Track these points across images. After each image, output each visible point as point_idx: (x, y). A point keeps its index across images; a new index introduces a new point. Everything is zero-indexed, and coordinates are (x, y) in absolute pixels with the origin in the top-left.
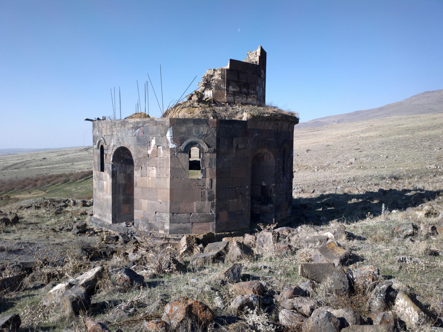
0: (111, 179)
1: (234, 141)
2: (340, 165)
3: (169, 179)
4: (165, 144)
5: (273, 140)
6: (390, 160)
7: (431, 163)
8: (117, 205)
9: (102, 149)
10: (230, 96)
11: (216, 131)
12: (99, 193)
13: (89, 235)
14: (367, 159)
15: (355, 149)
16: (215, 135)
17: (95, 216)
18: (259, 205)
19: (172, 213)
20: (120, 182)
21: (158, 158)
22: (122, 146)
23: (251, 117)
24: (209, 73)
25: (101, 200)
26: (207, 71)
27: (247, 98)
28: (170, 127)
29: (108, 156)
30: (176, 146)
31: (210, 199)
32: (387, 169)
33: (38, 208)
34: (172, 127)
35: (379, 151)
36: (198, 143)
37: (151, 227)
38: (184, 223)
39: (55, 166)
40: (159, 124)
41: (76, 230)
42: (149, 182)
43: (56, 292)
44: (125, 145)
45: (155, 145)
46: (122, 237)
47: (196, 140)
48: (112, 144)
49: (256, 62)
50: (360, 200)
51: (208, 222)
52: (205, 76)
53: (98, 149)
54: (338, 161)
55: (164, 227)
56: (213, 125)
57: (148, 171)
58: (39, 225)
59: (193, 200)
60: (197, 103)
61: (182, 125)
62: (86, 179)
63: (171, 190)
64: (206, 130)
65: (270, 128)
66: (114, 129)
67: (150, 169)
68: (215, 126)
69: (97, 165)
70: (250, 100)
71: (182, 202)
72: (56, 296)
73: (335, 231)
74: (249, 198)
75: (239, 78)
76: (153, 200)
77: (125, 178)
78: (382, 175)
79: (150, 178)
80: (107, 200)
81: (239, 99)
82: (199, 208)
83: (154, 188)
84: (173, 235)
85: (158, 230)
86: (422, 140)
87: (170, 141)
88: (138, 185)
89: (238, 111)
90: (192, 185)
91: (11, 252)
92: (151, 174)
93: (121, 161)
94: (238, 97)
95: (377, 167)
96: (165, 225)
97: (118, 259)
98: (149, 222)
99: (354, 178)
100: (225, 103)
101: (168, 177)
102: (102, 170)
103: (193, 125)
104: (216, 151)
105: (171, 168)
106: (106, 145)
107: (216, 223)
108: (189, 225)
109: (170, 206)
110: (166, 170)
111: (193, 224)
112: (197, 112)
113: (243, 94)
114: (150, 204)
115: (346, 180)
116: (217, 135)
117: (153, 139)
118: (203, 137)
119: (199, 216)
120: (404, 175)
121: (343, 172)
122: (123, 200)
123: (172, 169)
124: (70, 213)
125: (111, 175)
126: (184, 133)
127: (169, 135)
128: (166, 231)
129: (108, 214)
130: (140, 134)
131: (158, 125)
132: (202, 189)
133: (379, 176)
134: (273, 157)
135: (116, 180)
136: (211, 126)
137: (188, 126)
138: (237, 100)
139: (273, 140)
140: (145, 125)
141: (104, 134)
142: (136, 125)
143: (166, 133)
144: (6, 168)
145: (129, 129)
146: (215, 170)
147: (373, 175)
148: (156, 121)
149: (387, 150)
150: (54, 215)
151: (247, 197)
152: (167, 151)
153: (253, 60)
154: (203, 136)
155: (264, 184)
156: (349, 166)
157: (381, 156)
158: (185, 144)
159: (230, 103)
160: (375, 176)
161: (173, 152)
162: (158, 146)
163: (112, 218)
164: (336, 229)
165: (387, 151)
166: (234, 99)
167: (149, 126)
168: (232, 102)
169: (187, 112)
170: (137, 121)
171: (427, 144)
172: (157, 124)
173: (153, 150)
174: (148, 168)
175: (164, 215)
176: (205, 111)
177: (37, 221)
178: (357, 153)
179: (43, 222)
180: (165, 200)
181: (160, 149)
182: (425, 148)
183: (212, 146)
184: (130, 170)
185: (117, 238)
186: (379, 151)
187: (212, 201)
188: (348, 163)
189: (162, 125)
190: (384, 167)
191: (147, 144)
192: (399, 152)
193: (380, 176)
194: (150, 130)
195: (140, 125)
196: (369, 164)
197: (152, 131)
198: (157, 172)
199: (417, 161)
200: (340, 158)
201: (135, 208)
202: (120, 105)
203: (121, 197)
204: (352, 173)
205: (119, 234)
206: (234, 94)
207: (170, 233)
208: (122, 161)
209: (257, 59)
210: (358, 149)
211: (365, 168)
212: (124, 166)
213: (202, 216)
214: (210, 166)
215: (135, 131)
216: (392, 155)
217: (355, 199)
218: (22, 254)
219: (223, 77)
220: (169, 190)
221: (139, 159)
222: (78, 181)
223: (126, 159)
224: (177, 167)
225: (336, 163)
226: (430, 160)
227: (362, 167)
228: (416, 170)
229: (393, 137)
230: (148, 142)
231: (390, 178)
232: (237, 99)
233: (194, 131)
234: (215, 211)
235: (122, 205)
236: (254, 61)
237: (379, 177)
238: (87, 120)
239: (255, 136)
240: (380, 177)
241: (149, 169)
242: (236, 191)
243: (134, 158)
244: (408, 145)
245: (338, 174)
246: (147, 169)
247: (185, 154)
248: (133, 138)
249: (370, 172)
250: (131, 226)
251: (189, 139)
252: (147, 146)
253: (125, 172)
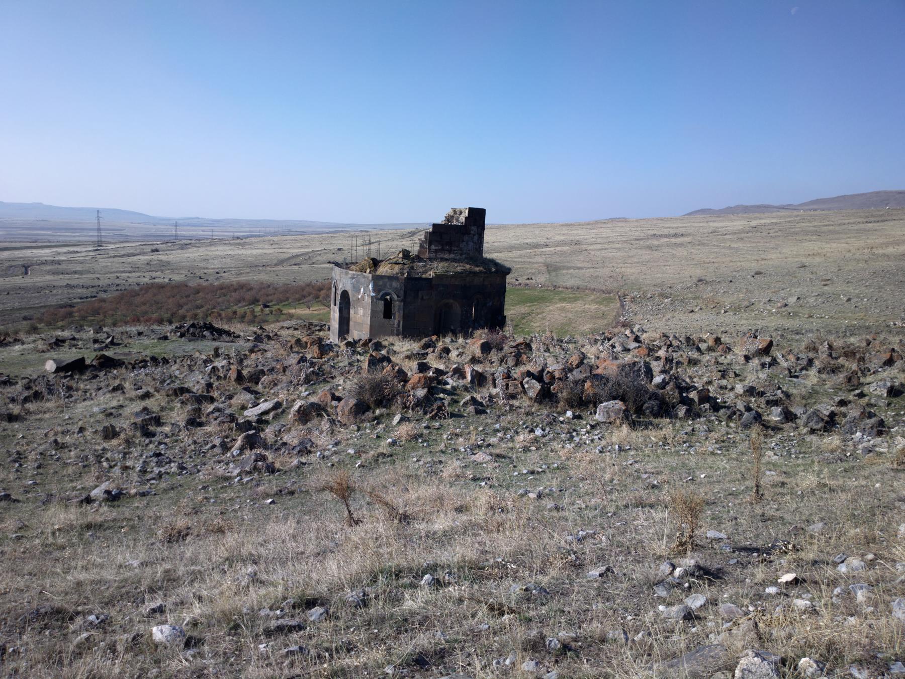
33: (296, 329)
47: (390, 291)
63: (371, 326)
65: (457, 283)
123: (372, 310)
144: (281, 262)
146: (402, 314)
206: (436, 251)
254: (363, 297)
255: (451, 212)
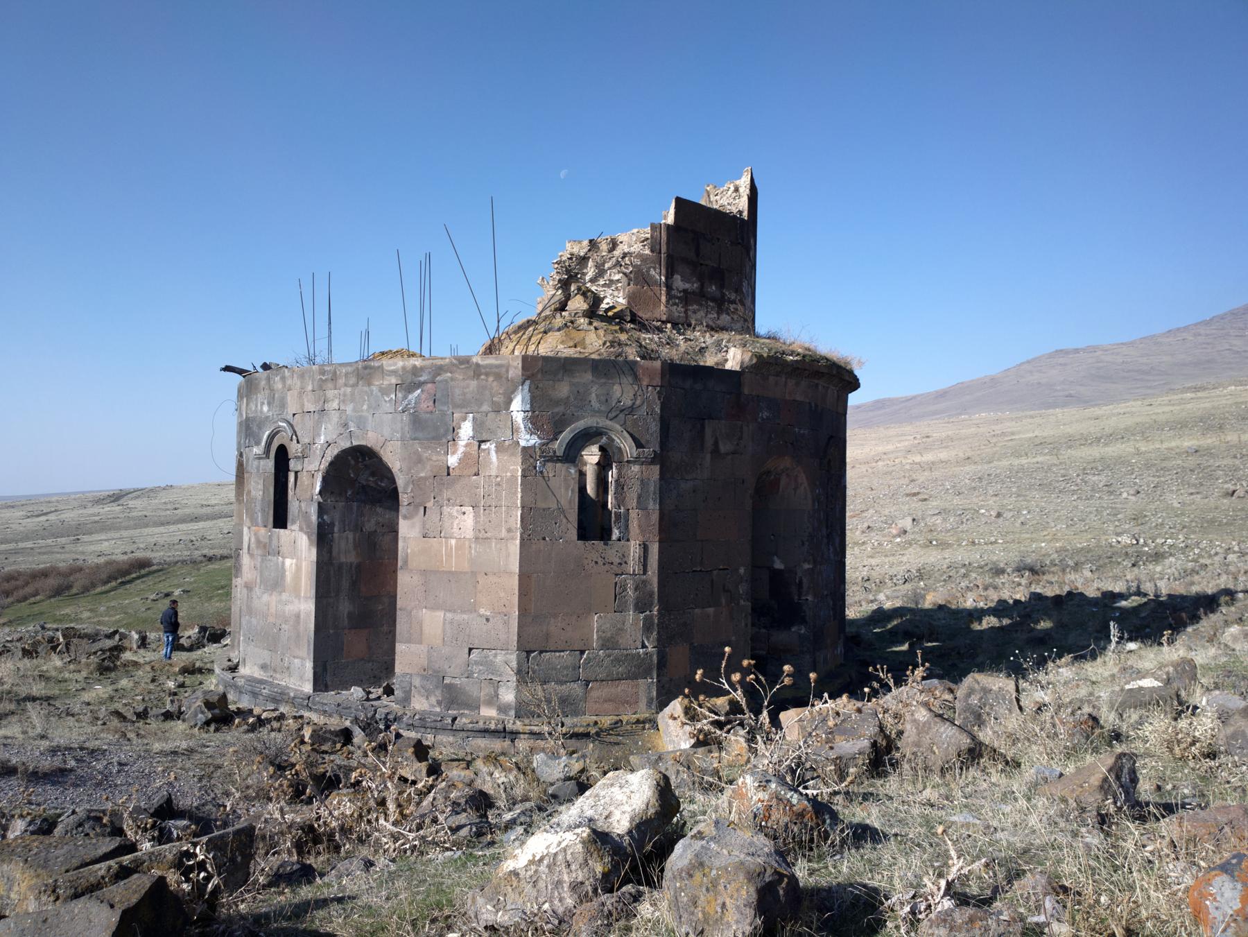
0: (314, 551)
1: (708, 432)
2: (875, 538)
3: (518, 542)
4: (505, 435)
5: (806, 432)
6: (1007, 523)
7: (1119, 530)
8: (331, 631)
9: (282, 457)
10: (675, 304)
11: (659, 399)
12: (266, 598)
13: (246, 727)
14: (944, 520)
15: (907, 495)
16: (658, 410)
17: (243, 671)
18: (765, 627)
19: (526, 650)
20: (343, 559)
21: (480, 480)
22: (355, 443)
23: (755, 361)
24: (575, 250)
25: (271, 619)
26: (568, 245)
27: (719, 314)
28: (523, 384)
29: (303, 477)
30: (539, 441)
31: (641, 607)
32: (1005, 546)
34: (528, 382)
35: (975, 500)
36: (606, 434)
37: (453, 697)
38: (562, 683)
39: (21, 545)
40: (487, 374)
41: (202, 712)
42: (449, 555)
43: (543, 868)
44: (370, 439)
45: (473, 437)
46: (364, 730)
47: (603, 422)
48: (322, 439)
49: (741, 212)
50: (1006, 622)
51: (634, 677)
52: (564, 259)
53: (268, 457)
54: (866, 525)
55: (497, 695)
56: (651, 379)
57: (445, 519)
58: (58, 704)
59: (589, 610)
60: (587, 320)
61: (560, 376)
62: (123, 583)
63: (524, 577)
64: (631, 395)
65: (799, 398)
66: (331, 393)
67: (455, 514)
68: (657, 381)
69: (258, 508)
70: (725, 318)
71: (555, 616)
72: (541, 884)
73: (1168, 673)
74: (745, 604)
75: (698, 254)
76: (463, 612)
77: (357, 546)
78: (994, 563)
79: (453, 542)
80: (298, 616)
81: (698, 314)
82: (609, 635)
83: (465, 573)
84: (527, 721)
85: (478, 708)
86: (1084, 469)
87: (522, 426)
88: (413, 564)
89: (704, 345)
90: (586, 562)
91: (36, 777)
92: (455, 530)
93: (346, 492)
94: (695, 307)
95: (977, 541)
96: (502, 691)
97: (496, 774)
98: (447, 681)
99: (919, 570)
100: (663, 322)
101: (513, 538)
102: (280, 520)
103: (591, 377)
104: (660, 459)
105: (523, 507)
106: (298, 442)
107: (659, 681)
108: (576, 688)
109: (520, 627)
110: (509, 515)
111: (588, 685)
112: (595, 341)
113: (708, 299)
114: (451, 623)
115: (899, 577)
116: (662, 410)
117: (464, 419)
118: (622, 416)
119: (607, 661)
120: (1053, 564)
121: (886, 556)
122: (350, 615)
124: (148, 668)
125: (314, 537)
126: (566, 402)
127: (518, 407)
128: (503, 709)
129: (296, 661)
130: (424, 406)
131: (483, 377)
132: (617, 575)
133: (987, 565)
134: (806, 484)
135: (330, 552)
136: (645, 383)
137: (576, 380)
138: (694, 316)
139: (806, 432)
140: (438, 378)
141: (292, 407)
142: (409, 379)
143: (509, 401)
145: (384, 391)
146: (655, 517)
147: (970, 564)
148: (478, 365)
149: (996, 495)
150: (96, 675)
151: (742, 602)
152: (513, 454)
153: (729, 207)
154: (622, 411)
155: (778, 565)
156: (898, 540)
157: (983, 511)
158: (566, 435)
159: (675, 325)
160: (976, 565)
161: (532, 460)
162: (481, 442)
163: (315, 674)
164: (1171, 669)
165: (994, 498)
166: (686, 312)
167: (452, 379)
168: (681, 320)
169: (562, 342)
170: (415, 367)
171: (1100, 480)
172: (479, 375)
173: (466, 455)
174: (446, 510)
175: (499, 658)
176: (617, 340)
177: (50, 693)
178: (915, 504)
179: (67, 694)
180: (504, 610)
181: (489, 449)
182: (1098, 492)
183: (648, 442)
184: (373, 521)
185: (346, 736)
186: (975, 500)
187: (648, 613)
188: (894, 532)
189: (498, 377)
190: (995, 542)
191: (445, 435)
192: (1028, 501)
193: (990, 566)
194: (457, 391)
195: (422, 379)
196: (952, 533)
197: (464, 394)
198: (476, 522)
199: (1080, 526)
200: (872, 516)
201: (398, 637)
202: (330, 328)
203: (345, 607)
204: (913, 558)
205: (351, 722)
206: (686, 298)
207: (518, 716)
208: (349, 493)
209: (743, 204)
210: (915, 494)
211: (943, 545)
212: (355, 508)
213: (617, 660)
214: (641, 505)
215: (405, 397)
216: (1010, 510)
217: (992, 618)
218: (76, 786)
219: (658, 247)
220: (517, 577)
221: (417, 483)
222: (99, 590)
223: (363, 487)
224: (542, 505)
225: (863, 532)
226: (1117, 523)
227: (934, 543)
228: (1082, 549)
229: (1005, 463)
230: (447, 431)
231: (1019, 571)
232: (695, 312)
233: (593, 395)
234: (655, 644)
235: (346, 631)
236: (735, 210)
237: (987, 568)
238: (228, 369)
239: (763, 419)
240: (991, 569)
241: (450, 515)
242: (712, 581)
243: (400, 482)
244: (1051, 484)
245: (873, 562)
246: (445, 513)
247: (566, 465)
248: (399, 417)
249: (961, 555)
250: (379, 698)
251: (578, 419)
252: (444, 440)
253: (358, 528)
254: (473, 463)
255: (581, 249)
